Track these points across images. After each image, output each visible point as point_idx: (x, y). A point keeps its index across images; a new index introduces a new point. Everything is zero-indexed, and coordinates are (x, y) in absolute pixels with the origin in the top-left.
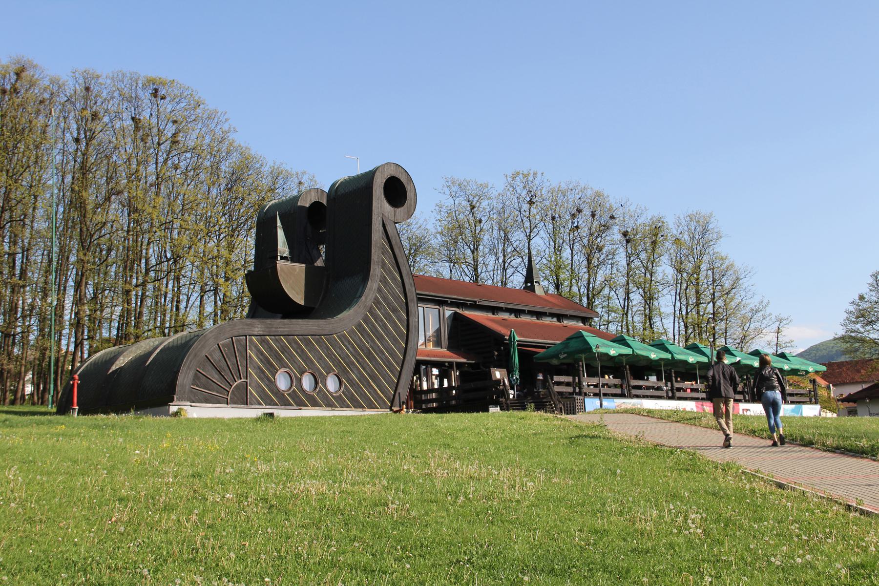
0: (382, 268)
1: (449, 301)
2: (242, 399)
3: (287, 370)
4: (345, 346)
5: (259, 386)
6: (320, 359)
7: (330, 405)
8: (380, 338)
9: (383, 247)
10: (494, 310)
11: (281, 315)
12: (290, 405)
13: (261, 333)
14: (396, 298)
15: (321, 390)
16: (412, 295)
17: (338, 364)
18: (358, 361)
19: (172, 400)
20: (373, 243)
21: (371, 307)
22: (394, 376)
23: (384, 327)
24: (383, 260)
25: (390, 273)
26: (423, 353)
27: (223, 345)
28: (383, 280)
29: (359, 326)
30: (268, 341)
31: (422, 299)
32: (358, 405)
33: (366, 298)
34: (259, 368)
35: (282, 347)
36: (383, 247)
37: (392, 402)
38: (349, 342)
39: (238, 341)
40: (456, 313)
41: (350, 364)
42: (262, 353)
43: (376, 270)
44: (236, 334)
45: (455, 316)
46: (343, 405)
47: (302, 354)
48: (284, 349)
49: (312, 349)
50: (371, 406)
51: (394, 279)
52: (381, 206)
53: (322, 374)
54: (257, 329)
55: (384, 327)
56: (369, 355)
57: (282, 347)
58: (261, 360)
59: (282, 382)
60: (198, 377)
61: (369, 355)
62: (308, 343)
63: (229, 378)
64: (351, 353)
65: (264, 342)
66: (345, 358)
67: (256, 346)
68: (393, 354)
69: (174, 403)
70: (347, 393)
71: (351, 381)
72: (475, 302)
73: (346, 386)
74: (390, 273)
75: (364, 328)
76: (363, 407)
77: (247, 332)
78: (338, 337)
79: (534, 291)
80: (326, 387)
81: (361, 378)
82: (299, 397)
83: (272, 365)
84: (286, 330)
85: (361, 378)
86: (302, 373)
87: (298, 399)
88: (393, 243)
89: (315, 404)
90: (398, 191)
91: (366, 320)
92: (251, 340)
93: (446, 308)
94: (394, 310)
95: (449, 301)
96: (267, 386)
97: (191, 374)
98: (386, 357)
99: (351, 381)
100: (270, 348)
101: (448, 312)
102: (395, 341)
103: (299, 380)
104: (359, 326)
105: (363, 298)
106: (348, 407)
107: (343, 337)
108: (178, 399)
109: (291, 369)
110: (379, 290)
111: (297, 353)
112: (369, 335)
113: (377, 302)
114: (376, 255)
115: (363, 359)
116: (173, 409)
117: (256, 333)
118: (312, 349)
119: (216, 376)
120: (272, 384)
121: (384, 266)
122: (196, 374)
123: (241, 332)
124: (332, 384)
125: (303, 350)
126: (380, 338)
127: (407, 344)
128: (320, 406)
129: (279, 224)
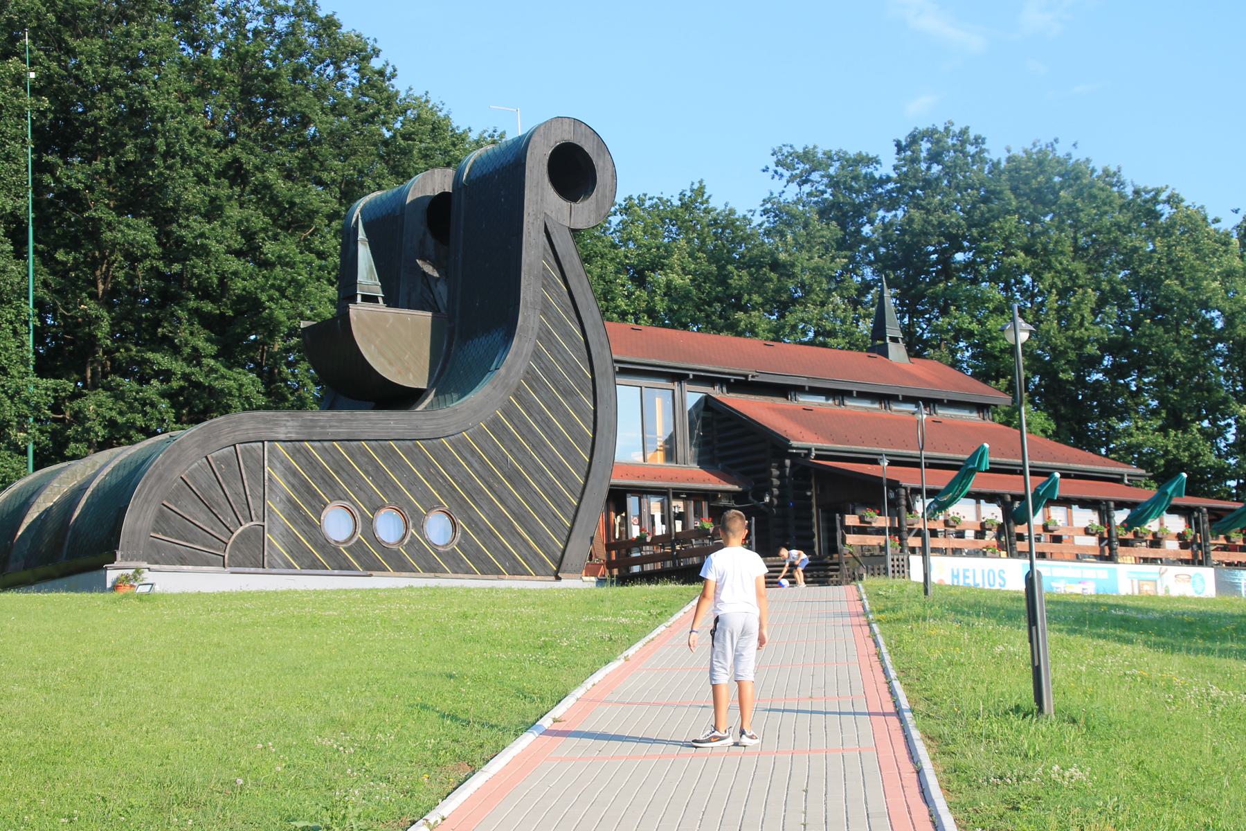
0: (544, 314)
1: (691, 374)
2: (251, 555)
3: (347, 504)
4: (465, 459)
5: (288, 530)
6: (413, 483)
7: (432, 568)
8: (538, 446)
9: (545, 275)
10: (783, 391)
11: (373, 404)
12: (350, 567)
13: (294, 436)
14: (573, 371)
15: (413, 540)
16: (603, 365)
17: (449, 493)
18: (490, 488)
19: (113, 559)
20: (524, 268)
21: (520, 387)
22: (565, 515)
23: (546, 424)
24: (546, 299)
25: (560, 325)
26: (629, 468)
27: (216, 459)
28: (545, 336)
29: (495, 425)
30: (307, 451)
31: (624, 372)
32: (488, 569)
33: (509, 370)
34: (290, 500)
35: (336, 462)
36: (545, 275)
37: (559, 563)
38: (473, 452)
39: (245, 451)
41: (475, 493)
42: (295, 473)
43: (529, 318)
44: (244, 438)
45: (708, 404)
46: (458, 568)
47: (377, 474)
48: (340, 466)
49: (397, 465)
50: (516, 571)
51: (568, 335)
52: (541, 201)
53: (417, 510)
54: (283, 430)
55: (546, 424)
56: (514, 477)
57: (336, 462)
59: (337, 524)
60: (162, 521)
61: (514, 477)
62: (389, 455)
63: (229, 520)
64: (476, 472)
65: (295, 453)
66: (466, 482)
67: (283, 462)
68: (562, 474)
69: (116, 564)
71: (473, 523)
72: (746, 376)
73: (464, 532)
74: (560, 325)
75: (504, 427)
76: (499, 572)
77: (265, 435)
78: (450, 443)
79: (885, 353)
80: (423, 536)
81: (497, 517)
82: (368, 553)
83: (314, 495)
84: (343, 431)
85: (497, 517)
86: (375, 509)
87: (366, 556)
89: (401, 566)
90: (575, 169)
91: (509, 412)
92: (273, 451)
93: (686, 386)
94: (567, 393)
95: (691, 374)
96: (304, 532)
97: (151, 513)
98: (549, 479)
99: (473, 523)
100: (311, 464)
101: (693, 396)
102: (568, 451)
103: (369, 523)
104: (495, 425)
105: (502, 370)
106: (468, 571)
107: (461, 446)
108: (125, 558)
109: (353, 503)
110: (537, 355)
111: (366, 473)
112: (515, 440)
113: (530, 377)
114: (529, 289)
115: (501, 483)
116: (112, 575)
117: (282, 437)
118: (397, 465)
119: (202, 516)
120: (313, 529)
121: (546, 309)
122: (161, 511)
123: (252, 435)
124: (437, 529)
125: (378, 467)
126: (538, 446)
127: (591, 458)
128: (413, 570)
129: (362, 234)
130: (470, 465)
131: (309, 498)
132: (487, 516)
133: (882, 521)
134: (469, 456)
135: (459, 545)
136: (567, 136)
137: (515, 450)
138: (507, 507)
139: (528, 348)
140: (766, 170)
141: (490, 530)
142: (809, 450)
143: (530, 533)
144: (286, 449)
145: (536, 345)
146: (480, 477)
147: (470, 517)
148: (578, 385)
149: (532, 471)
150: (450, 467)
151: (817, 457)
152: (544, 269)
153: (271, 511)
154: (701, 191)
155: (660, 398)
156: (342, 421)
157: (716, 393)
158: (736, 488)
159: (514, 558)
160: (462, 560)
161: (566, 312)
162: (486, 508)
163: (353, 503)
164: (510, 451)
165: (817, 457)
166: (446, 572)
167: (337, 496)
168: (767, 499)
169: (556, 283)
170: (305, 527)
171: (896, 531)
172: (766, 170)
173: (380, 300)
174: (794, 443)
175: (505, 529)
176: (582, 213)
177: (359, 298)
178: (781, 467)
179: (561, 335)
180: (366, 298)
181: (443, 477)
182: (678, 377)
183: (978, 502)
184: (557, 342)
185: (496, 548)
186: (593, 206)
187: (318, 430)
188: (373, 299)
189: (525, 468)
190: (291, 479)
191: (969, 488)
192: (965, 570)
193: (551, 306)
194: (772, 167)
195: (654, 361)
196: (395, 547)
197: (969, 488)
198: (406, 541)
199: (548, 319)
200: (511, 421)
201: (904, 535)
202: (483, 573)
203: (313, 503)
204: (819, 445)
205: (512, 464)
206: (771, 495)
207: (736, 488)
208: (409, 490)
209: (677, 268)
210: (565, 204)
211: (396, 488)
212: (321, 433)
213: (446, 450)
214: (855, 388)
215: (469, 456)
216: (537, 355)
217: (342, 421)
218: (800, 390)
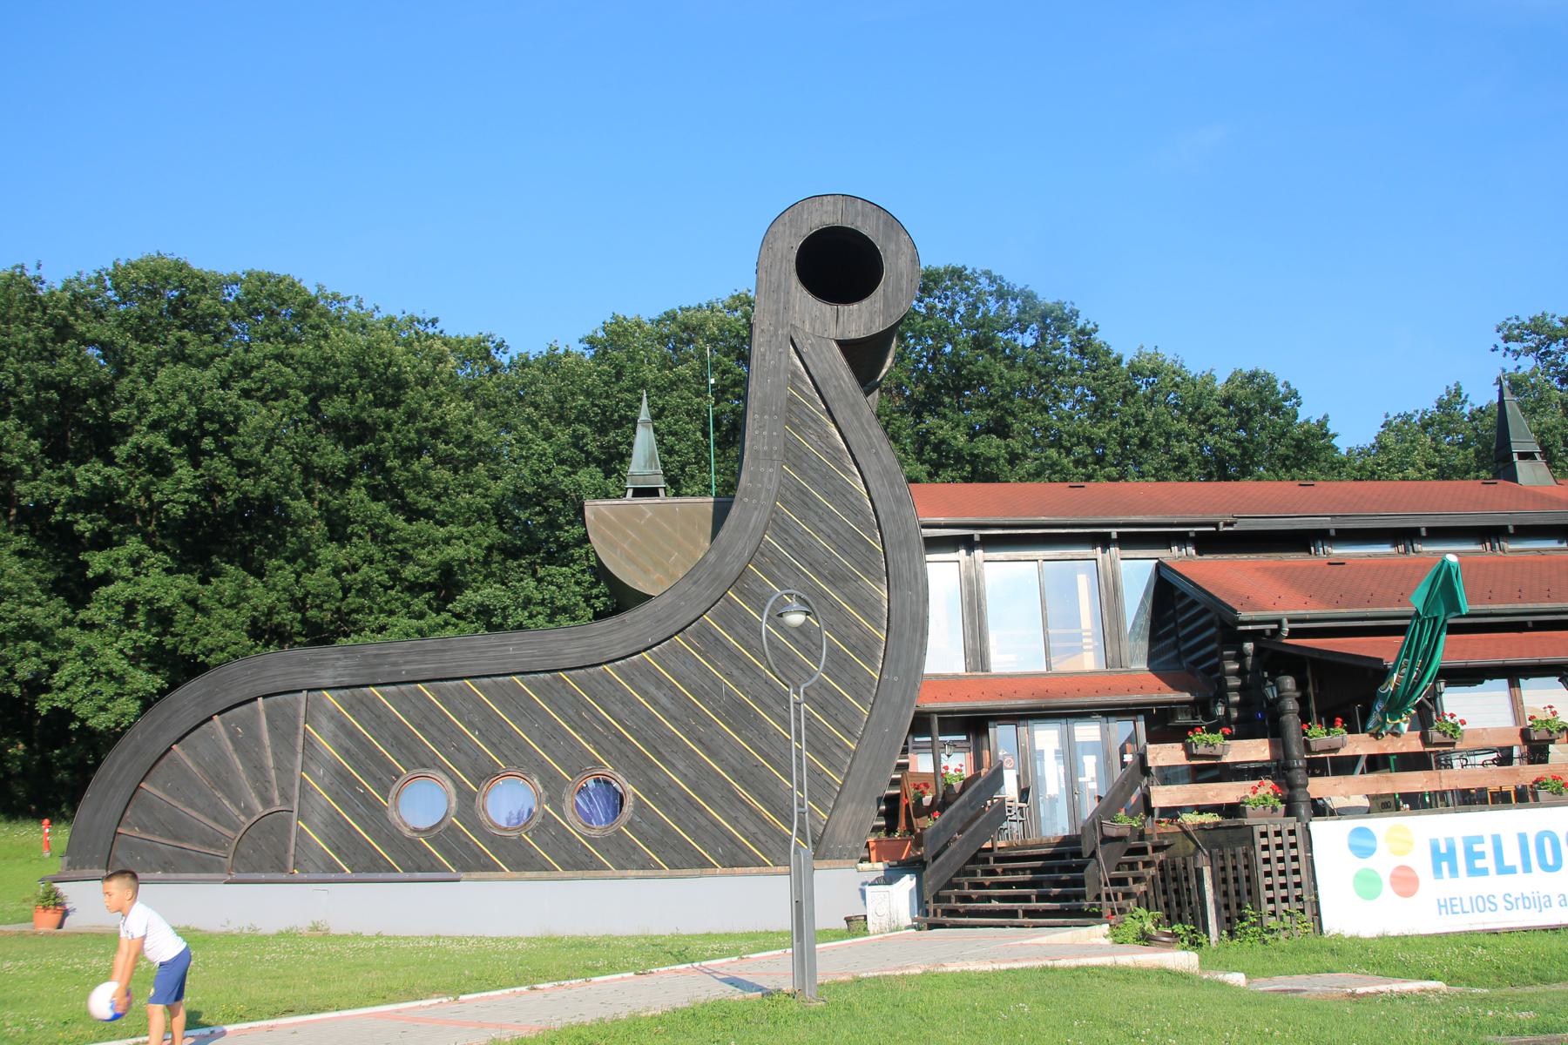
0: (794, 466)
1: (1114, 532)
4: (644, 693)
6: (549, 736)
10: (1300, 540)
13: (347, 681)
32: (682, 860)
38: (660, 682)
40: (1160, 567)
41: (661, 744)
42: (351, 733)
48: (428, 719)
49: (523, 710)
54: (330, 672)
56: (738, 715)
58: (347, 753)
70: (644, 824)
72: (1216, 525)
77: (300, 682)
78: (619, 670)
82: (467, 845)
84: (429, 667)
85: (701, 779)
86: (485, 774)
88: (831, 394)
94: (837, 578)
95: (1114, 532)
100: (379, 720)
106: (646, 864)
115: (709, 723)
120: (374, 815)
121: (795, 456)
123: (281, 685)
125: (490, 716)
130: (654, 702)
131: (373, 768)
132: (684, 777)
133: (1257, 750)
134: (652, 689)
135: (630, 825)
136: (828, 217)
137: (736, 672)
138: (719, 762)
139: (757, 518)
140: (1495, 348)
141: (688, 798)
142: (1279, 622)
143: (763, 799)
144: (341, 701)
145: (775, 511)
146: (672, 719)
147: (650, 781)
148: (858, 564)
149: (770, 702)
150: (617, 708)
151: (1294, 633)
152: (791, 399)
153: (304, 788)
154: (1458, 393)
155: (1079, 572)
156: (426, 652)
157: (1173, 555)
158: (1187, 696)
159: (732, 839)
160: (635, 848)
161: (833, 459)
162: (681, 766)
163: (446, 770)
164: (729, 676)
165: (1294, 633)
166: (603, 867)
167: (420, 762)
168: (1220, 711)
169: (816, 421)
170: (362, 810)
171: (1278, 771)
172: (1495, 348)
173: (661, 492)
174: (1244, 615)
175: (715, 795)
176: (860, 319)
177: (630, 492)
178: (1240, 657)
179: (826, 494)
180: (639, 493)
181: (604, 723)
182: (1103, 541)
183: (1514, 684)
184: (817, 503)
185: (698, 826)
186: (879, 305)
187: (387, 668)
188: (653, 492)
189: (755, 699)
190: (348, 743)
191: (1439, 661)
192: (1469, 842)
193: (807, 454)
194: (1502, 345)
195: (1043, 519)
196: (514, 835)
197: (1439, 661)
198: (533, 824)
199: (803, 474)
200: (729, 628)
201: (1299, 776)
202: (672, 866)
203: (379, 774)
204: (1301, 612)
205: (729, 693)
206: (1228, 706)
207: (1187, 696)
208: (544, 747)
209: (1422, 465)
210: (827, 309)
211: (522, 747)
212: (390, 674)
213: (610, 680)
214: (1423, 524)
215: (652, 689)
216: (779, 526)
217: (426, 652)
218: (1322, 536)
